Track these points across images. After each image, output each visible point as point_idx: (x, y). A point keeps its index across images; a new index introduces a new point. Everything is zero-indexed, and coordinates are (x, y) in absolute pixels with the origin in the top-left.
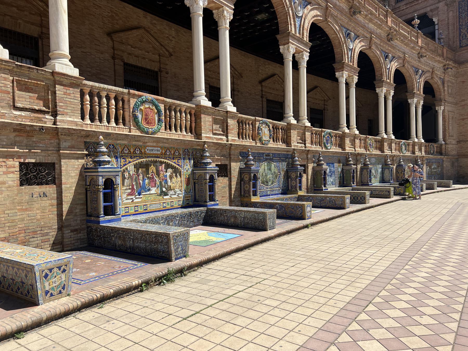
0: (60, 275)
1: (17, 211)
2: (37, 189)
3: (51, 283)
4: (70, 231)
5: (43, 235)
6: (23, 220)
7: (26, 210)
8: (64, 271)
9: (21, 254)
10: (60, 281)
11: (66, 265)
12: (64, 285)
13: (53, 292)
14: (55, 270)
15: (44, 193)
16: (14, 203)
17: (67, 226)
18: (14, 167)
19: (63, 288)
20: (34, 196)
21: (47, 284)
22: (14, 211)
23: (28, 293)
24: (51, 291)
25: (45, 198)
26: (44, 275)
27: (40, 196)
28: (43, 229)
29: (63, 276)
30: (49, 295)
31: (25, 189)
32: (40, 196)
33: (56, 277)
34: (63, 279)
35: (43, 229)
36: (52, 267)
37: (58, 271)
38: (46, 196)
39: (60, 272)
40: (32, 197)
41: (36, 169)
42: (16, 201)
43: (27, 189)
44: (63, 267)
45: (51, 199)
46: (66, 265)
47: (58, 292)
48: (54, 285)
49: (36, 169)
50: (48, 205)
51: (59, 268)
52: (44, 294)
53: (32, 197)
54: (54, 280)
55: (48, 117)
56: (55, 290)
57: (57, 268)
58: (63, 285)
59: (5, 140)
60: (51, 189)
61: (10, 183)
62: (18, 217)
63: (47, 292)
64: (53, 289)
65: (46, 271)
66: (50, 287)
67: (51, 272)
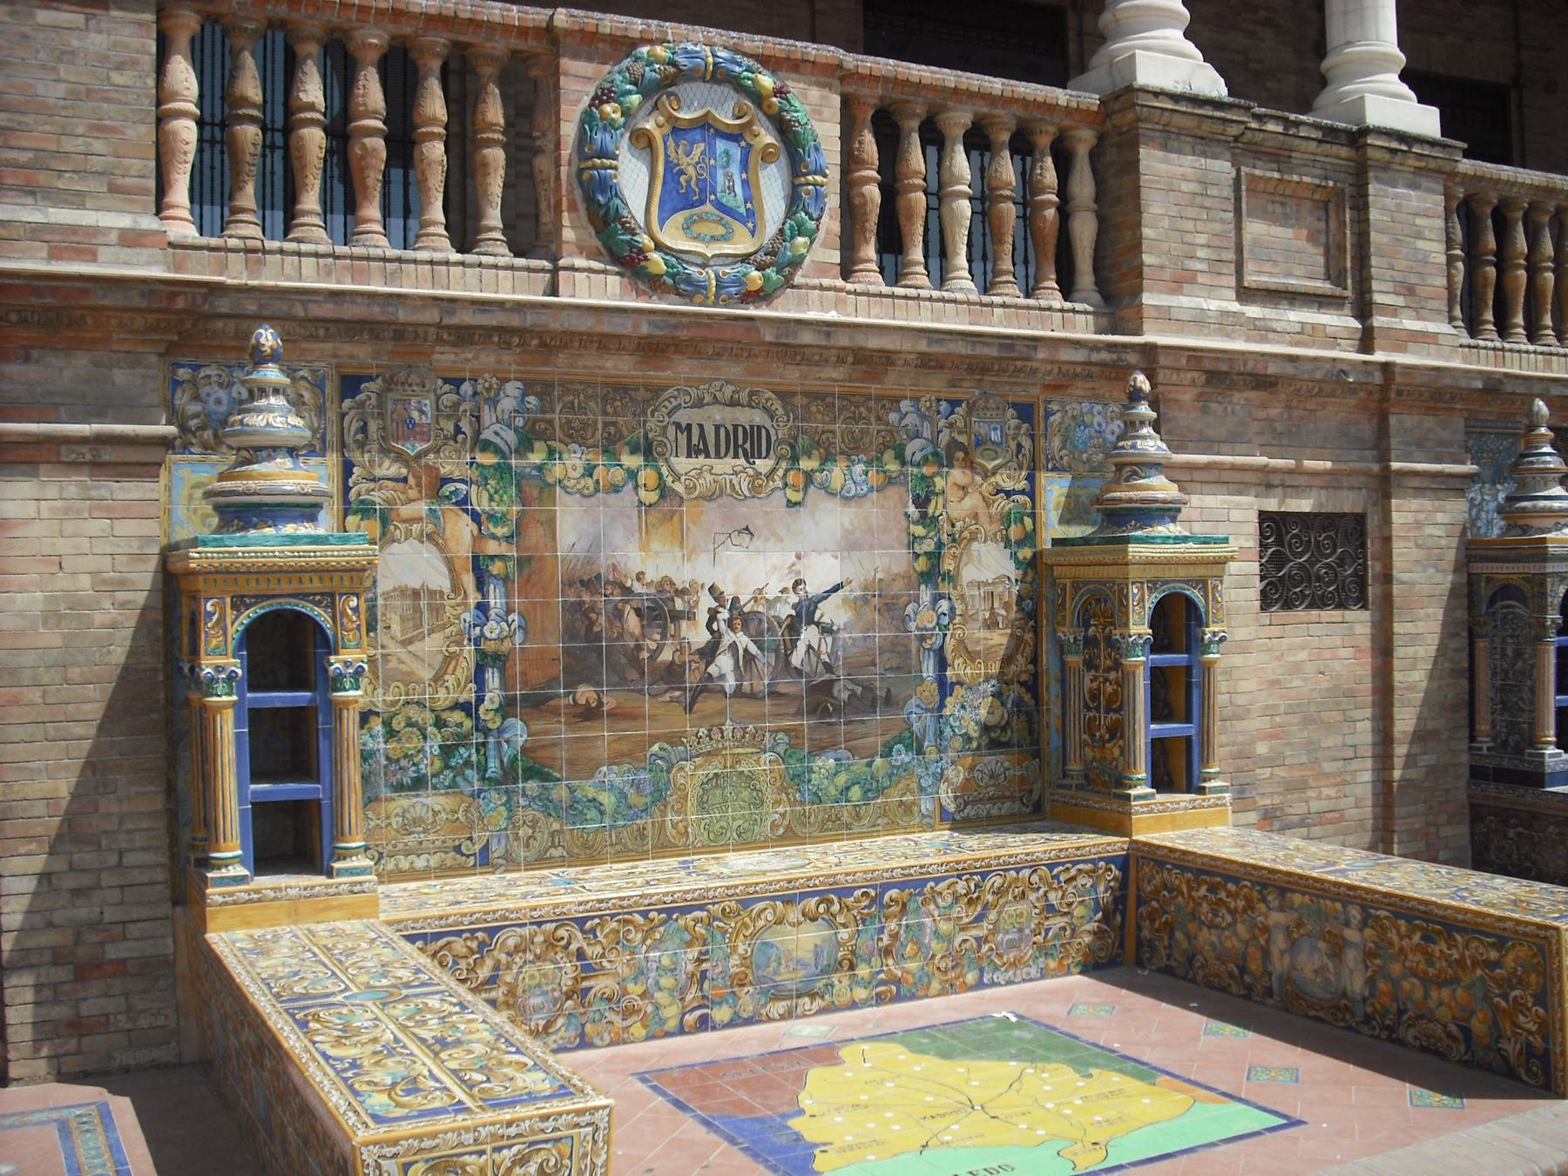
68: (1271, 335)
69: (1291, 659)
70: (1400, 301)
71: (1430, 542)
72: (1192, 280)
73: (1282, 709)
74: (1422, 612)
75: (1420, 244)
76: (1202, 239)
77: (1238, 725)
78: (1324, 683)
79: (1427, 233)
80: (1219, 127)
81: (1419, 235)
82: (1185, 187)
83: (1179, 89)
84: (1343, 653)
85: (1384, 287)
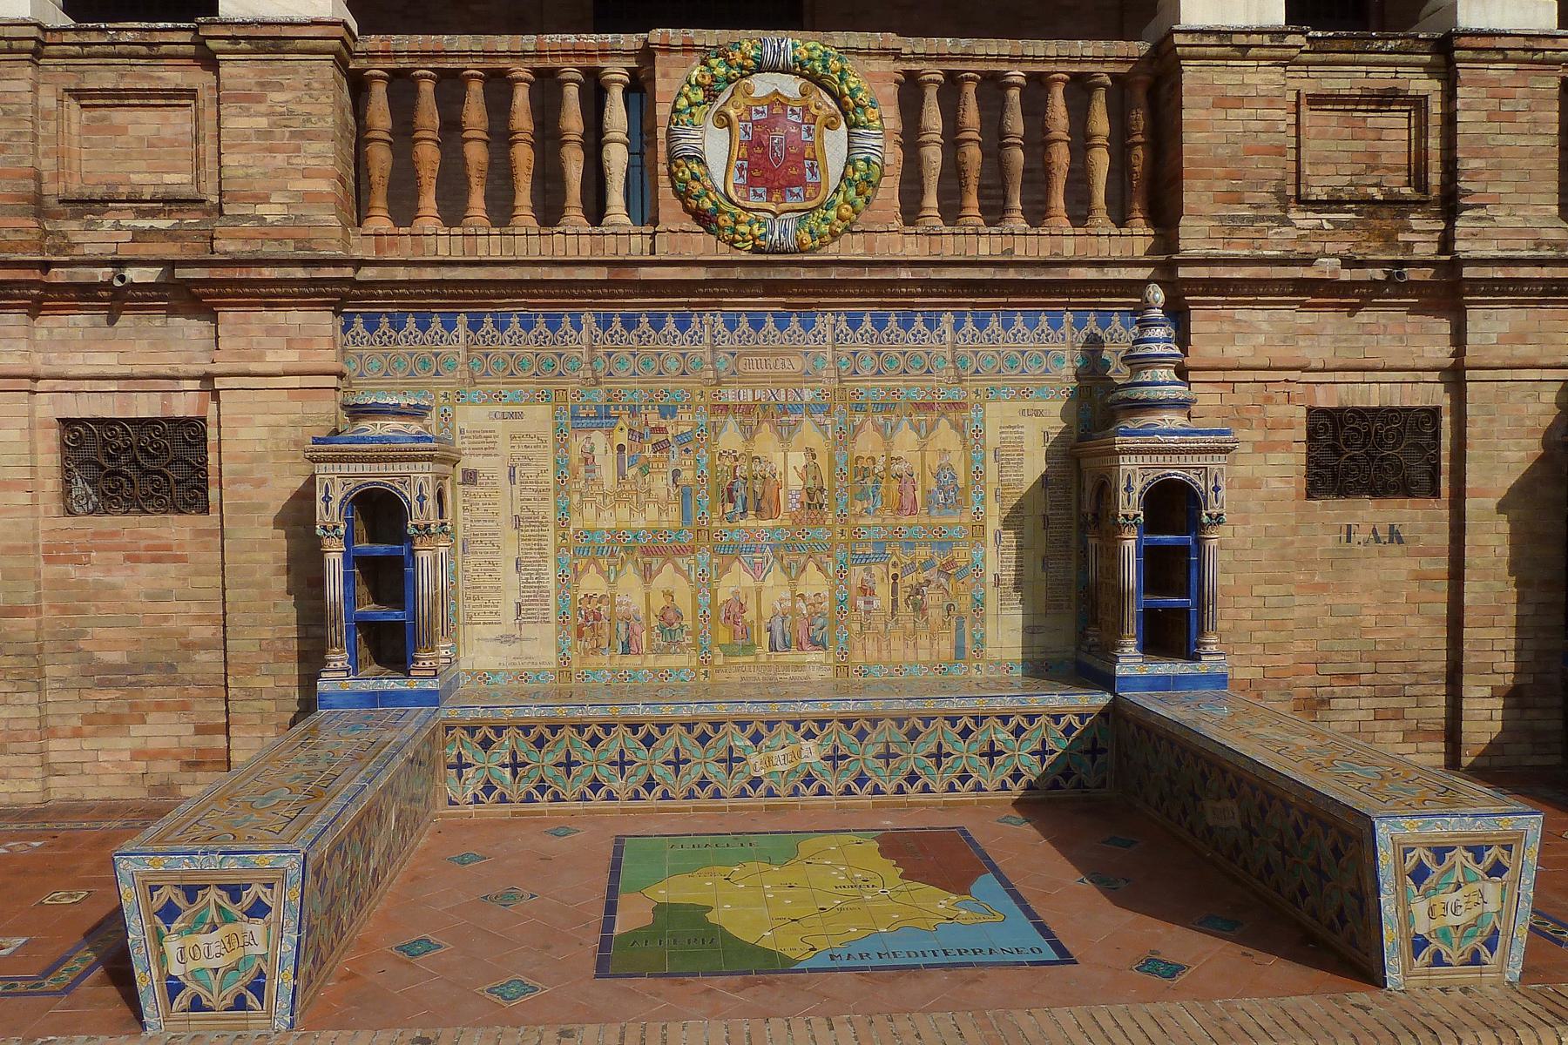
0: (1477, 886)
1: (1292, 590)
2: (1368, 513)
3: (1438, 910)
4: (1488, 691)
5: (1382, 691)
6: (1312, 623)
7: (1324, 587)
8: (1497, 870)
9: (1317, 759)
10: (1477, 911)
11: (1509, 848)
12: (1495, 932)
13: (1444, 949)
14: (1460, 857)
15: (1392, 526)
16: (1283, 558)
17: (1480, 671)
18: (1290, 427)
19: (1491, 945)
20: (1356, 537)
21: (1420, 908)
22: (1281, 590)
23: (1343, 922)
24: (1435, 944)
25: (1395, 549)
26: (1410, 865)
27: (1378, 540)
28: (1382, 667)
29: (1492, 889)
30: (1426, 955)
31: (1325, 507)
32: (1378, 540)
33: (1459, 887)
34: (1492, 906)
35: (1382, 667)
36: (1447, 842)
37: (1471, 865)
38: (1400, 541)
39: (1479, 870)
40: (1349, 540)
41: (1368, 434)
42: (1290, 551)
43: (1334, 510)
44: (1494, 851)
45: (1423, 553)
46: (1509, 848)
47: (1467, 956)
48: (1452, 920)
49: (1368, 434)
50: (1403, 575)
51: (1478, 852)
52: (1406, 948)
53: (1349, 540)
54: (1451, 898)
55: (1415, 220)
56: (1455, 942)
57: (1468, 849)
58: (1487, 930)
59: (1265, 326)
60: (1421, 518)
61: (1275, 484)
62: (1298, 613)
63: (1419, 944)
64: (1444, 934)
65: (1420, 852)
66: (1434, 924)
67: (1440, 861)
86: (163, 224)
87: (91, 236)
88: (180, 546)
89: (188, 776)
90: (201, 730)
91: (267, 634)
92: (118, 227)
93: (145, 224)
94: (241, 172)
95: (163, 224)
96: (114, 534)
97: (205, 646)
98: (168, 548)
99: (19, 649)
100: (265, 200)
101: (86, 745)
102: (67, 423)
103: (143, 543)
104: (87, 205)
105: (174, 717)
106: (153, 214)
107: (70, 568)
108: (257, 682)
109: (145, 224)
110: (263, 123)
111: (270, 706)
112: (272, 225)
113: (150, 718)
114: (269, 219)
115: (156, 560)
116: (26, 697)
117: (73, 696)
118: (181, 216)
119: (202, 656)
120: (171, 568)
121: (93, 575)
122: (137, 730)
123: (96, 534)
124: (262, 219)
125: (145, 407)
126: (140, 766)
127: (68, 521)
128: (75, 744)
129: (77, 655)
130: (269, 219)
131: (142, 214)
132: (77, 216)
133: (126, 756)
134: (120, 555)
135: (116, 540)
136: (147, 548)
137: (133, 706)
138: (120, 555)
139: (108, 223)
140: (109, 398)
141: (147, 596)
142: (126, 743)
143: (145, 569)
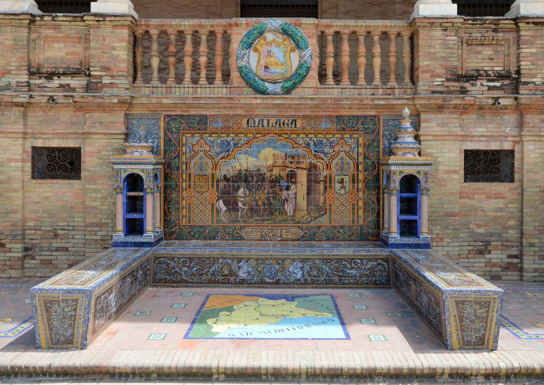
68: (45, 89)
69: (44, 195)
70: (104, 73)
71: (104, 157)
72: (9, 72)
73: (40, 211)
74: (100, 182)
75: (115, 52)
76: (14, 59)
77: (13, 215)
78: (60, 203)
79: (118, 48)
80: (19, 21)
81: (114, 49)
82: (7, 43)
83: (7, 11)
84: (68, 194)
85: (95, 69)
86: (498, 84)
87: (474, 88)
88: (505, 193)
89: (504, 273)
90: (509, 257)
91: (537, 224)
92: (482, 85)
93: (491, 84)
94: (527, 67)
95: (498, 84)
96: (483, 189)
97: (511, 228)
98: (501, 194)
99: (453, 227)
100: (535, 76)
101: (471, 260)
102: (466, 151)
103: (492, 193)
104: (472, 77)
105: (500, 252)
106: (493, 81)
107: (467, 200)
108: (533, 241)
109: (491, 84)
110: (534, 50)
111: (537, 249)
112: (539, 85)
113: (492, 252)
114: (537, 83)
115: (497, 198)
116: (455, 244)
117: (467, 244)
118: (502, 81)
119: (510, 231)
120: (501, 201)
121: (474, 203)
122: (487, 256)
123: (477, 189)
124: (533, 83)
125: (494, 146)
126: (488, 269)
127: (466, 184)
128: (467, 260)
129: (468, 230)
130: (537, 83)
131: (489, 81)
132: (467, 81)
133: (484, 265)
134: (484, 196)
135: (484, 191)
136: (494, 194)
137: (486, 248)
138: (484, 196)
139: (478, 83)
140: (482, 143)
141: (493, 210)
142: (484, 261)
143: (492, 201)
